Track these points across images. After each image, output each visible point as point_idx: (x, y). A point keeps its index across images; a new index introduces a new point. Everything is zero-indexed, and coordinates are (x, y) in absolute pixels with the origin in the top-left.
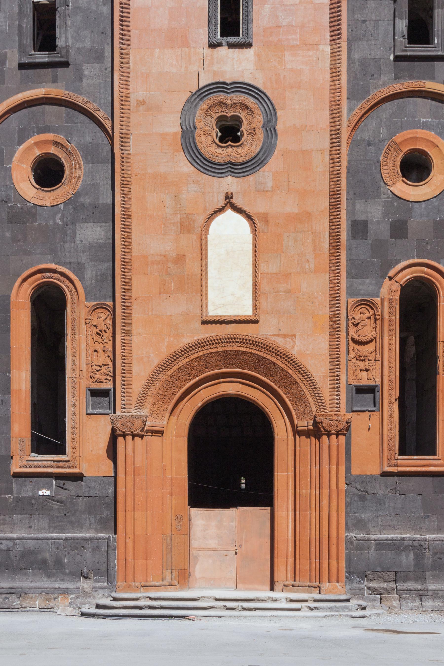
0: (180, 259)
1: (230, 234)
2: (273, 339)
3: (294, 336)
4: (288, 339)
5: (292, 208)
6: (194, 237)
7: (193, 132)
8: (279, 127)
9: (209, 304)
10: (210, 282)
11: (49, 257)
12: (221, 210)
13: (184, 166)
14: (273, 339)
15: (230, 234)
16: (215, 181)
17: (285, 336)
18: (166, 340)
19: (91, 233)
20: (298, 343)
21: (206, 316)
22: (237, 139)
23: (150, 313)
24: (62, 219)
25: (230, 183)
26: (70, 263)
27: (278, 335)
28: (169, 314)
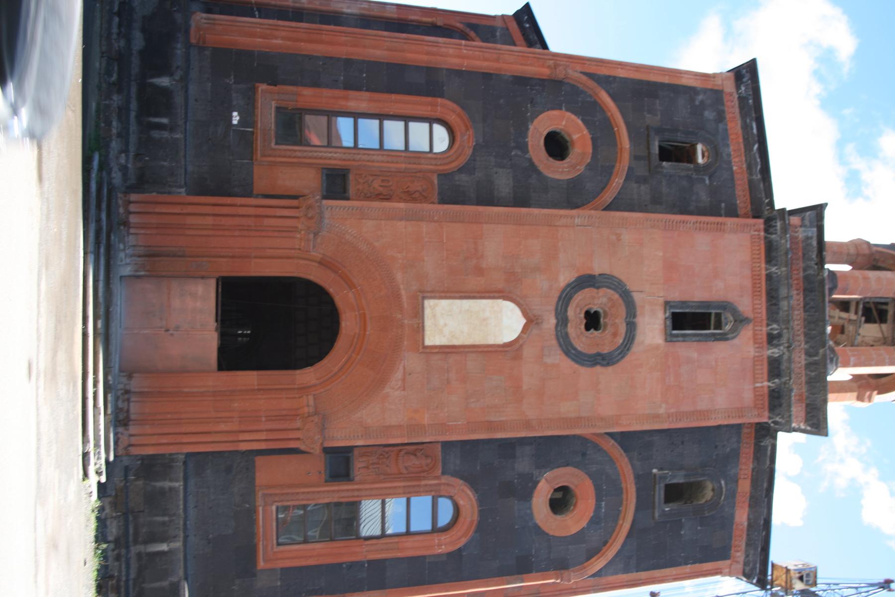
0: (479, 271)
1: (504, 322)
2: (401, 368)
3: (404, 390)
4: (400, 383)
5: (528, 382)
6: (500, 285)
7: (593, 286)
8: (598, 369)
9: (436, 301)
10: (458, 302)
11: (481, 140)
12: (525, 314)
13: (565, 278)
14: (401, 368)
15: (504, 322)
16: (552, 307)
17: (404, 380)
18: (399, 255)
19: (504, 182)
20: (397, 393)
21: (424, 298)
22: (588, 328)
23: (426, 240)
24: (516, 155)
25: (551, 321)
26: (475, 160)
27: (404, 373)
28: (426, 258)
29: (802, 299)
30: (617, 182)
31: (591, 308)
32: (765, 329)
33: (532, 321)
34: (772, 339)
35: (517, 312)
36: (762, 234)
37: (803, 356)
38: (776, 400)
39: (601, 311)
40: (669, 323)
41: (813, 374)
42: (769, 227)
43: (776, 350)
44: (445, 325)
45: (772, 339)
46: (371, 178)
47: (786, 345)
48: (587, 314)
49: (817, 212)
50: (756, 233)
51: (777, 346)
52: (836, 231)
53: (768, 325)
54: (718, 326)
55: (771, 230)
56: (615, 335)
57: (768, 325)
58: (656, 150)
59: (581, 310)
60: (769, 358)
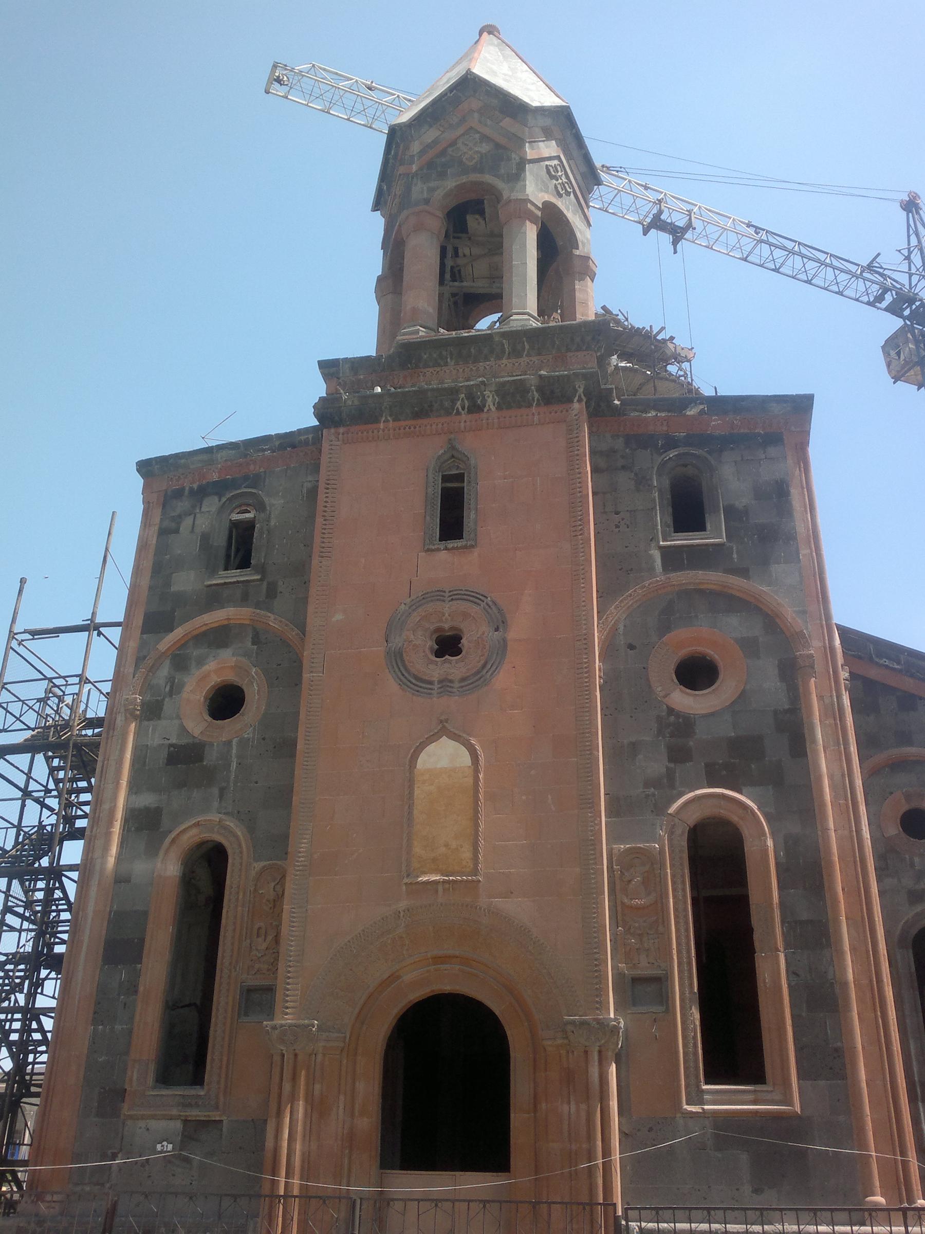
29: (431, 370)
30: (273, 621)
31: (431, 648)
32: (464, 416)
33: (443, 730)
34: (476, 408)
35: (431, 748)
36: (341, 430)
37: (504, 361)
38: (554, 394)
39: (435, 637)
40: (451, 544)
41: (527, 347)
43: (490, 400)
44: (447, 845)
45: (476, 408)
46: (254, 952)
47: (483, 387)
48: (439, 654)
51: (484, 401)
53: (458, 413)
54: (460, 477)
56: (465, 615)
57: (458, 413)
58: (235, 575)
59: (432, 662)
60: (499, 408)
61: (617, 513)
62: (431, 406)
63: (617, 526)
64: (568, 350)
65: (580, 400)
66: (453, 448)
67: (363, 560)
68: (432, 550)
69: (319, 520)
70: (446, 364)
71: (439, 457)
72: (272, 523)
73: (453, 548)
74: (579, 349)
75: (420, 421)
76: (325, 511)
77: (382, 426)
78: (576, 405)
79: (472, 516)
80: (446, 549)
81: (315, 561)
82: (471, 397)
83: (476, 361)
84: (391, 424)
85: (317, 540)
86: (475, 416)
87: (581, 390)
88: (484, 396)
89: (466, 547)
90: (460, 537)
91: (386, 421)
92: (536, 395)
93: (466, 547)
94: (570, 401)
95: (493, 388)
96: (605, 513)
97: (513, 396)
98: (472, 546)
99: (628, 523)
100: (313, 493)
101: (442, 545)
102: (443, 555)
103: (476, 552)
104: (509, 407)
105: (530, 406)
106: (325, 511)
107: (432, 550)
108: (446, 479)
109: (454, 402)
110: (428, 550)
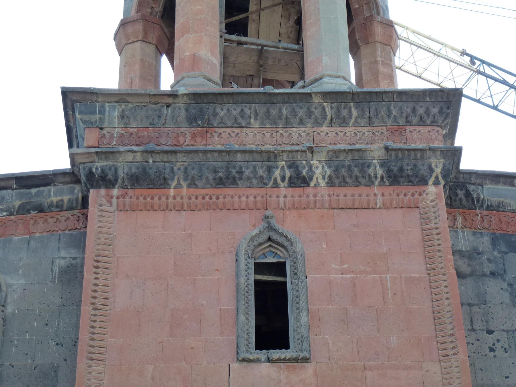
29: (229, 130)
32: (284, 189)
34: (299, 180)
36: (115, 192)
37: (325, 129)
40: (276, 354)
41: (355, 113)
42: (105, 181)
43: (318, 172)
47: (309, 155)
49: (75, 101)
50: (114, 201)
52: (104, 71)
53: (276, 185)
54: (279, 268)
55: (110, 176)
60: (331, 183)
61: (490, 332)
62: (241, 173)
63: (492, 350)
64: (408, 122)
65: (436, 183)
66: (271, 228)
67: (150, 368)
68: (249, 361)
69: (86, 309)
70: (249, 125)
71: (252, 239)
72: (9, 309)
73: (279, 360)
74: (422, 122)
75: (225, 191)
76: (95, 298)
77: (172, 192)
78: (431, 189)
79: (304, 318)
80: (269, 360)
81: (81, 365)
82: (292, 165)
83: (288, 124)
84: (184, 191)
85: (84, 337)
86: (298, 191)
87: (438, 171)
88: (311, 167)
89: (296, 360)
90: (286, 346)
91: (179, 186)
92: (380, 172)
93: (296, 360)
94: (424, 182)
95: (323, 156)
96: (473, 330)
97: (349, 170)
98: (306, 360)
99: (506, 346)
100: (72, 275)
101: (262, 354)
102: (265, 368)
103: (310, 368)
104: (344, 183)
105: (370, 183)
106: (95, 298)
107: (249, 361)
108: (260, 268)
109: (270, 170)
110: (244, 360)
